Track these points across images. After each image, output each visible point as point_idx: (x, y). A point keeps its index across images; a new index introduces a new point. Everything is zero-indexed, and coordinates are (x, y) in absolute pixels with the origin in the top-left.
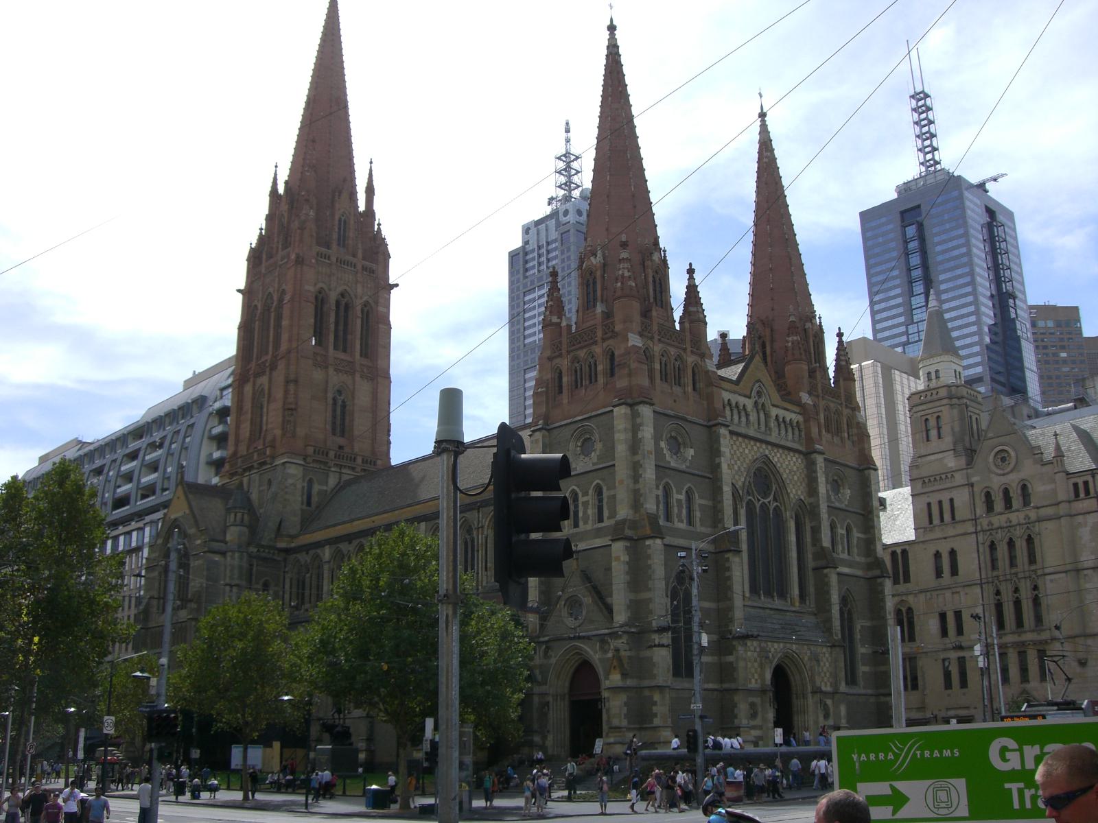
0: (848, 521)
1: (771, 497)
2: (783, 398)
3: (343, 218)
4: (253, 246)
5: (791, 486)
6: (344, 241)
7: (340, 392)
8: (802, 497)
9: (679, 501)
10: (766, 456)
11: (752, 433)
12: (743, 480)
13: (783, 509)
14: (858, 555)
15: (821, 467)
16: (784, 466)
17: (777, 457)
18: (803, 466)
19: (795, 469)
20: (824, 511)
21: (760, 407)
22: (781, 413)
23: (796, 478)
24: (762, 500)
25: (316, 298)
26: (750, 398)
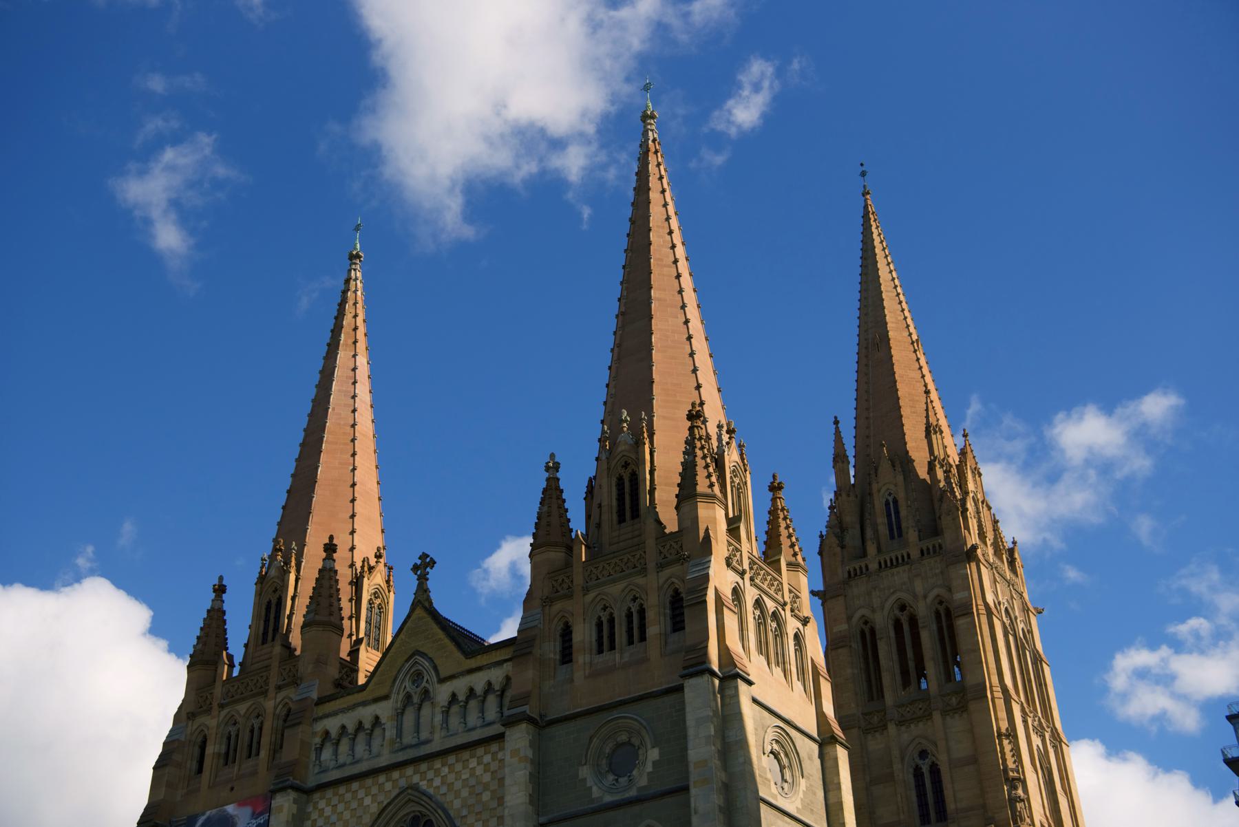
2: (468, 655)
3: (890, 499)
6: (899, 528)
7: (923, 754)
10: (415, 788)
11: (383, 761)
15: (515, 753)
16: (458, 785)
17: (432, 780)
22: (460, 686)
25: (863, 633)
26: (386, 697)
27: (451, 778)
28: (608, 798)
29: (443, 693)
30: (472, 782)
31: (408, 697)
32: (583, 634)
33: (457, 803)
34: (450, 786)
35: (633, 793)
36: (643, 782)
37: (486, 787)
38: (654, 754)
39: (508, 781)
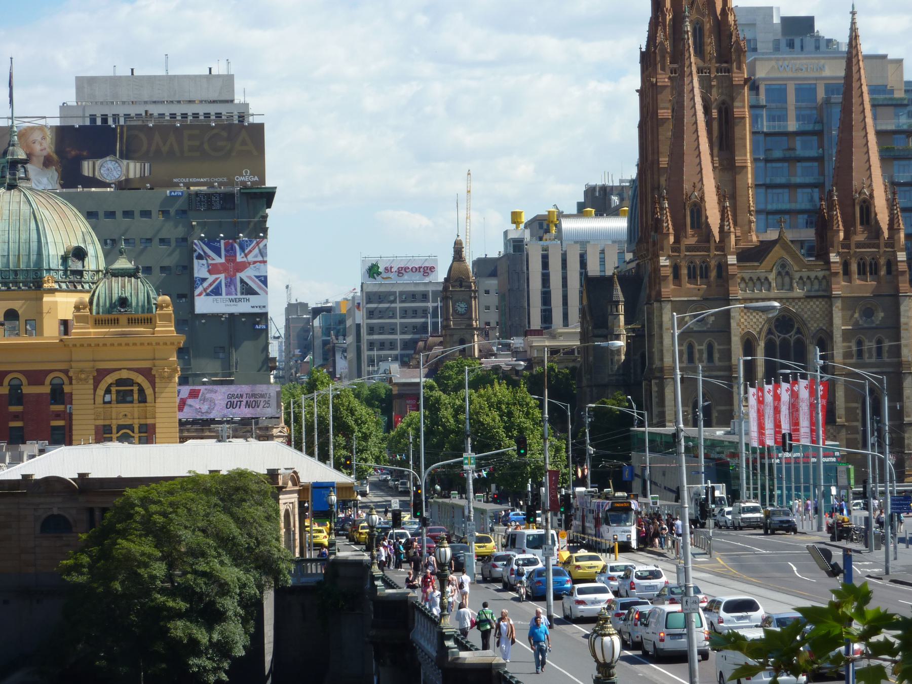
0: (879, 335)
1: (793, 333)
4: (644, 50)
5: (812, 322)
8: (824, 328)
9: (700, 351)
12: (760, 327)
13: (804, 338)
14: (888, 358)
15: (837, 307)
16: (806, 310)
18: (827, 306)
19: (818, 310)
20: (839, 336)
21: (783, 274)
23: (818, 316)
24: (783, 336)
27: (802, 307)
28: (866, 325)
29: (797, 276)
30: (812, 310)
31: (779, 274)
32: (854, 267)
33: (806, 316)
34: (803, 310)
35: (874, 325)
36: (878, 322)
37: (818, 313)
38: (882, 314)
39: (834, 316)
